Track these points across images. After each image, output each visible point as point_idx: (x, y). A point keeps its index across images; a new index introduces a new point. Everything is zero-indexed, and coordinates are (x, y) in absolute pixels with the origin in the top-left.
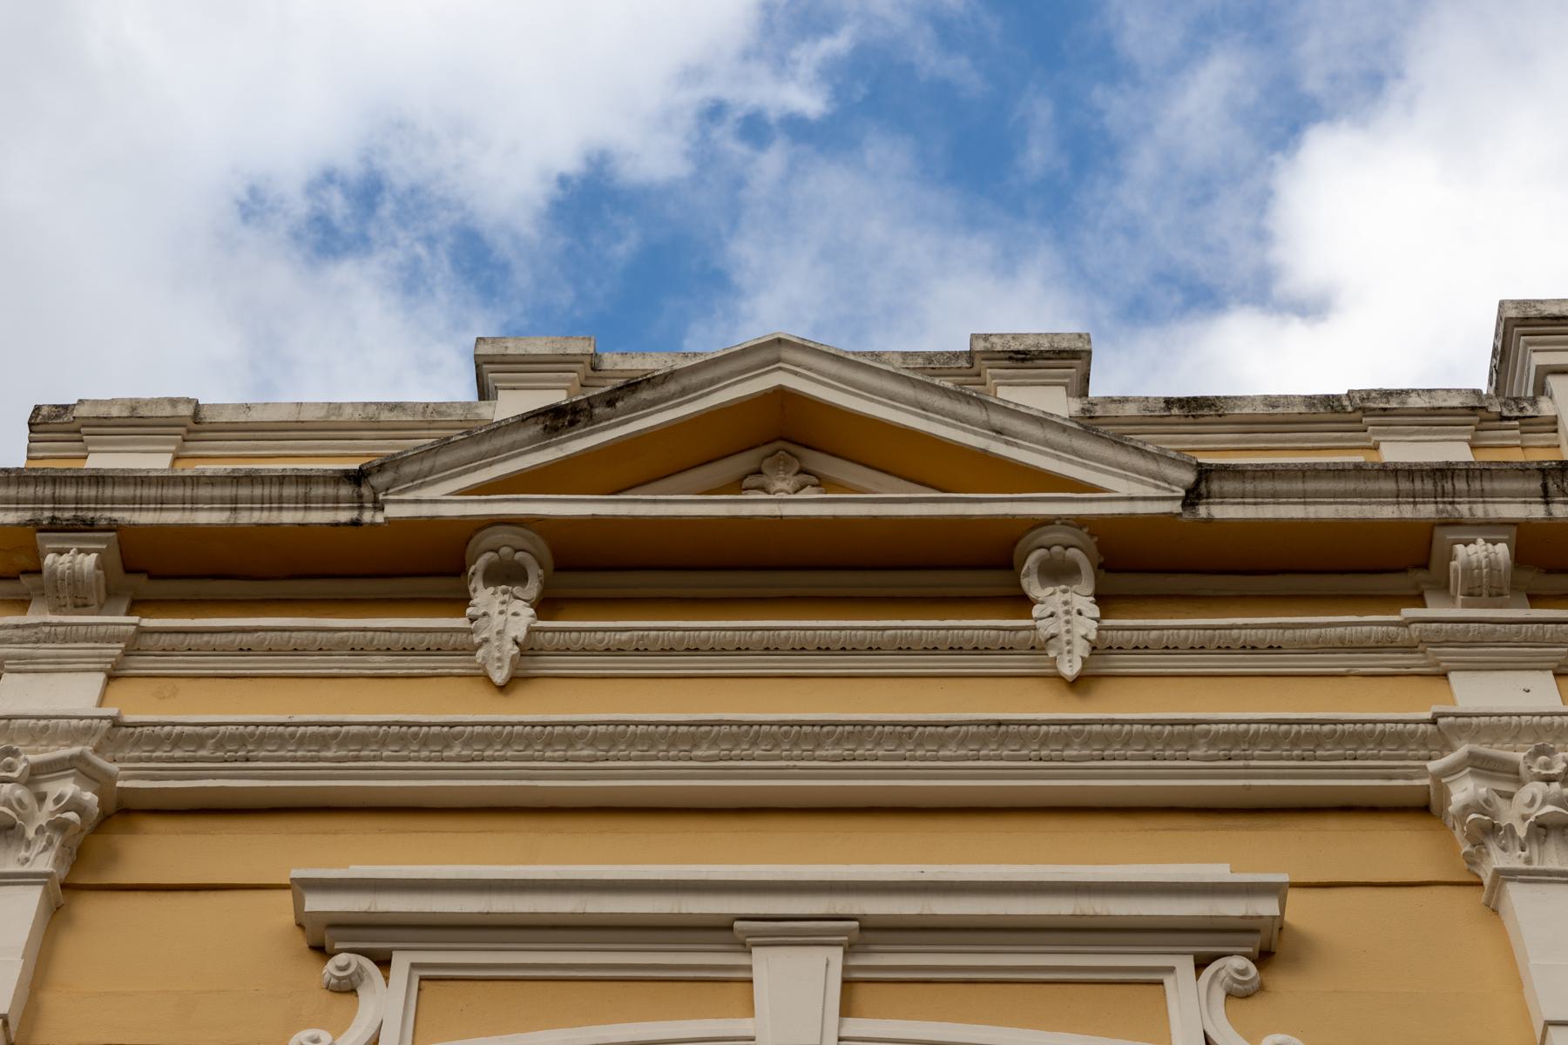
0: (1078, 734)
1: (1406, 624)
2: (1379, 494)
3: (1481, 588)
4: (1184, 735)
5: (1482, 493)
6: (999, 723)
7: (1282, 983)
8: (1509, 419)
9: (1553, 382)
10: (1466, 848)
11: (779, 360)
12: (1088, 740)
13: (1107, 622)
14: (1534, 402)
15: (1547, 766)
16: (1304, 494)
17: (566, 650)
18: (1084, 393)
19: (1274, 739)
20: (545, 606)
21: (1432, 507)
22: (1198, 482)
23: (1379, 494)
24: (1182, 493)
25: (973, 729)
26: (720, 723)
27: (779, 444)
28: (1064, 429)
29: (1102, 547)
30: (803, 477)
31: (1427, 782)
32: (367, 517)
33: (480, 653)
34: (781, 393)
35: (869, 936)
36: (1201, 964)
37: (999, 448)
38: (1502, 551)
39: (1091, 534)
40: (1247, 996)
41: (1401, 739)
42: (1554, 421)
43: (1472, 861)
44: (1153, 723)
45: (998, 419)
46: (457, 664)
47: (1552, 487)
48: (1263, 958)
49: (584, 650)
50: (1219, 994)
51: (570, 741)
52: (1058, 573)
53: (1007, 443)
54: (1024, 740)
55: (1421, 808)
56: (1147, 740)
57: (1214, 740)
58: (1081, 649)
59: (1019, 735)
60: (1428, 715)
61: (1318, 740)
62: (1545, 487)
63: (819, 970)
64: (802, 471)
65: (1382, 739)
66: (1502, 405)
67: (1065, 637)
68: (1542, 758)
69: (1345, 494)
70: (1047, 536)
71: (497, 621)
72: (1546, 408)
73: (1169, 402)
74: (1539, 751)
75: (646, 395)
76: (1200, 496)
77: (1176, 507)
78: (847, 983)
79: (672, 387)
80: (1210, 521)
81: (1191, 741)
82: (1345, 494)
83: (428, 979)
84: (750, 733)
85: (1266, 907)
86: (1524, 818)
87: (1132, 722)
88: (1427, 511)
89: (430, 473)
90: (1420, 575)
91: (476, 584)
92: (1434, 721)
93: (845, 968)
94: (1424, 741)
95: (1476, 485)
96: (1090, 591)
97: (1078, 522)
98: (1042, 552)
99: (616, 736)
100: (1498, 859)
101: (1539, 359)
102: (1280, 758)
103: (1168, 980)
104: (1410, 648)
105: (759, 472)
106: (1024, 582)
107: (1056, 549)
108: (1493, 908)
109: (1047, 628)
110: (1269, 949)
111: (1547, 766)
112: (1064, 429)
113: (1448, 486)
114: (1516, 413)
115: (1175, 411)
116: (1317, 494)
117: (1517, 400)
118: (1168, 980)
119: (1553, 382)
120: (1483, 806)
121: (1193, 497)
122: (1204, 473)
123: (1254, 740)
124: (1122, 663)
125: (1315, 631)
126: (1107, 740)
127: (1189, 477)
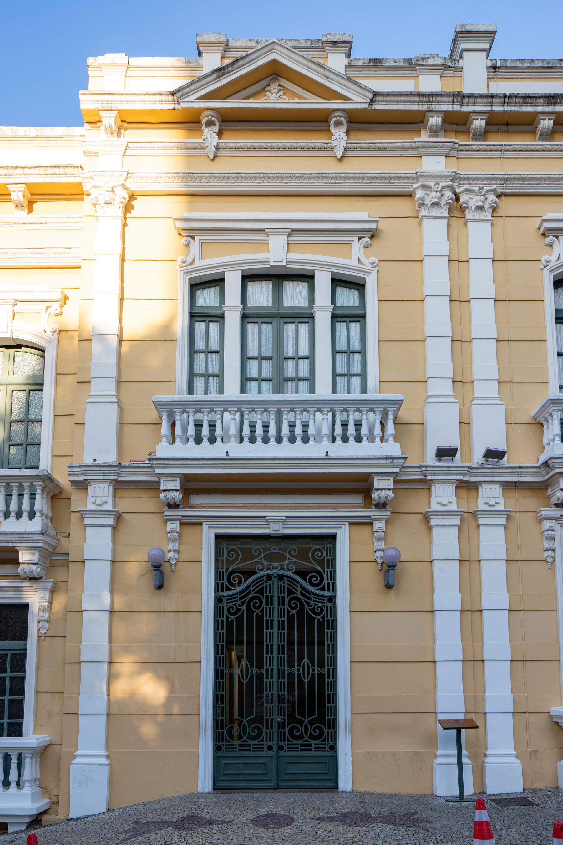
0: (339, 177)
1: (415, 142)
2: (415, 102)
3: (434, 132)
4: (361, 177)
5: (439, 102)
6: (322, 174)
7: (375, 242)
8: (451, 67)
9: (465, 54)
10: (417, 208)
11: (274, 49)
12: (341, 178)
13: (349, 141)
14: (458, 61)
15: (437, 188)
16: (398, 101)
17: (225, 148)
18: (349, 56)
19: (381, 178)
20: (220, 134)
21: (426, 106)
22: (373, 98)
23: (415, 102)
24: (369, 101)
25: (316, 175)
26: (261, 173)
27: (274, 76)
28: (343, 78)
29: (349, 116)
30: (280, 87)
31: (412, 189)
32: (177, 106)
33: (207, 149)
34: (274, 61)
35: (293, 232)
36: (360, 239)
37: (327, 83)
38: (440, 120)
39: (347, 113)
40: (368, 247)
41: (408, 178)
42: (462, 68)
43: (418, 211)
44: (356, 174)
45: (328, 74)
46: (201, 153)
47: (455, 100)
48: (372, 237)
49: (230, 149)
50: (362, 246)
51: (228, 178)
52: (338, 124)
53: (329, 81)
54: (327, 178)
55: (410, 195)
56: (354, 178)
57: (369, 178)
58: (342, 150)
59: (326, 177)
60: (415, 172)
61: (390, 178)
62: (453, 100)
63: (282, 240)
64: (279, 85)
65: (404, 178)
66: (451, 62)
67: (339, 146)
68: (437, 186)
69: (407, 102)
70: (336, 114)
71: (210, 139)
72: (461, 64)
73: (370, 60)
74: (437, 184)
75: (241, 63)
76: (373, 102)
77: (366, 106)
78: (288, 243)
79: (247, 60)
80: (374, 110)
81: (363, 178)
82: (407, 102)
83: (203, 243)
84: (268, 176)
85: (373, 226)
86: (430, 201)
87: (351, 173)
88: (425, 107)
89: (190, 92)
90: (421, 125)
91: (204, 127)
92: (416, 174)
93: (288, 240)
94: (413, 179)
95: (438, 99)
96: (345, 131)
97: (343, 110)
98: (335, 119)
99: (239, 177)
100: (423, 212)
101: (463, 46)
102: (382, 183)
103: (352, 243)
104: (415, 149)
105: (269, 85)
106: (330, 127)
107: (339, 118)
108: (420, 224)
109: (335, 143)
110: (373, 235)
111: (437, 188)
112: (343, 78)
113: (431, 99)
114: (453, 66)
115: (371, 64)
116: (400, 101)
117: (454, 60)
118: (352, 243)
119: (465, 54)
120: (422, 199)
121: (372, 102)
122: (375, 94)
123: (377, 178)
124: (350, 153)
125: (394, 144)
126: (345, 178)
127: (371, 96)
